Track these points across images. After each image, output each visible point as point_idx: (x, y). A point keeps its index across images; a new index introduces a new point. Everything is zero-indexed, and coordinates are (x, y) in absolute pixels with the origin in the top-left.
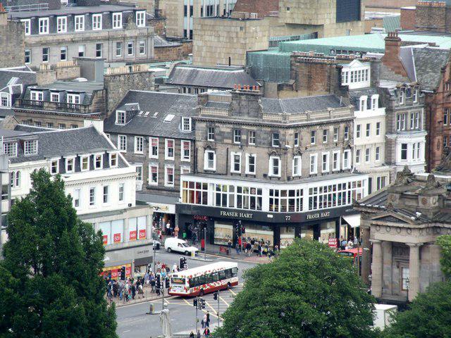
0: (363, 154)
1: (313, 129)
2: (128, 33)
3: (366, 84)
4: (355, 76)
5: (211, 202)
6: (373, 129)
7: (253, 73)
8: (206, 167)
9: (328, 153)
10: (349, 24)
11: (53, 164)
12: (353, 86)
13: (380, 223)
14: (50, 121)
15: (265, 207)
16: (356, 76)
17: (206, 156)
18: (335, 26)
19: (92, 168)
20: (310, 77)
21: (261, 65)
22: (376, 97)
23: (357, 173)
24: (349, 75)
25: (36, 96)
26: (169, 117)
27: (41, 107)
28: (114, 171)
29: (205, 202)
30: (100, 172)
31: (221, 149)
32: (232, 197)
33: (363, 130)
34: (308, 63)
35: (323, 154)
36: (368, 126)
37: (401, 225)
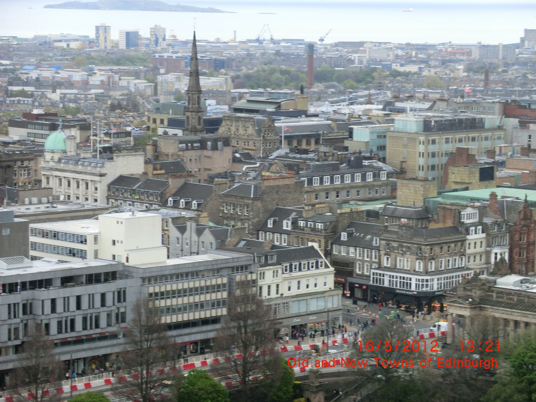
0: (472, 259)
1: (441, 246)
2: (375, 183)
3: (476, 220)
4: (469, 216)
5: (386, 284)
6: (478, 244)
7: (426, 210)
8: (385, 265)
9: (451, 259)
10: (487, 182)
11: (286, 267)
12: (466, 221)
13: (451, 304)
14: (307, 237)
15: (413, 288)
16: (469, 215)
17: (385, 259)
18: (479, 183)
19: (308, 269)
20: (444, 217)
21: (431, 205)
22: (480, 227)
23: (468, 269)
24: (466, 216)
25: (302, 223)
26: (369, 237)
27: (303, 230)
28: (322, 270)
29: (383, 284)
30: (313, 271)
31: (393, 255)
32: (397, 281)
33: (472, 245)
34: (444, 208)
35: (448, 259)
36: (475, 243)
37: (462, 306)
